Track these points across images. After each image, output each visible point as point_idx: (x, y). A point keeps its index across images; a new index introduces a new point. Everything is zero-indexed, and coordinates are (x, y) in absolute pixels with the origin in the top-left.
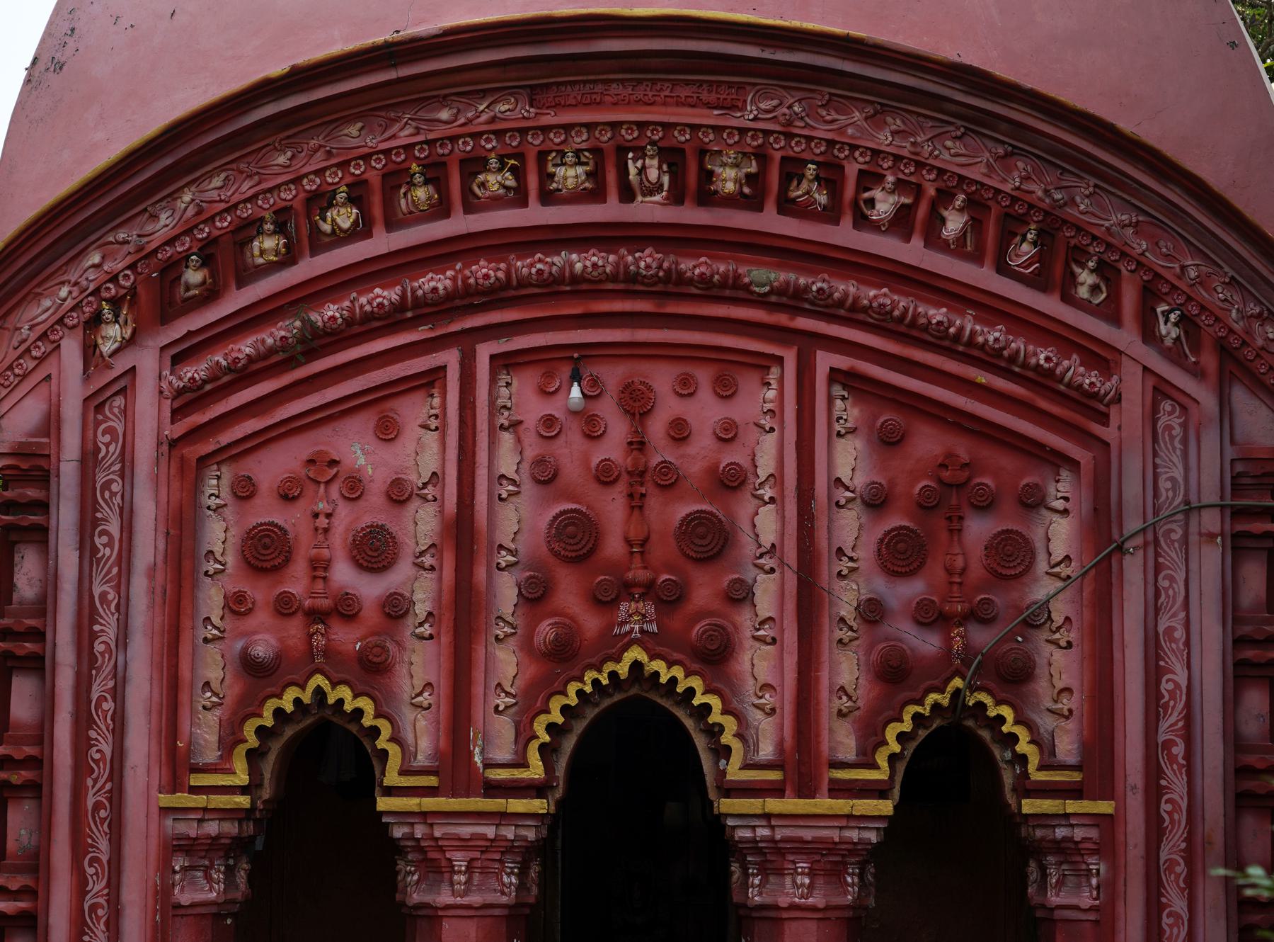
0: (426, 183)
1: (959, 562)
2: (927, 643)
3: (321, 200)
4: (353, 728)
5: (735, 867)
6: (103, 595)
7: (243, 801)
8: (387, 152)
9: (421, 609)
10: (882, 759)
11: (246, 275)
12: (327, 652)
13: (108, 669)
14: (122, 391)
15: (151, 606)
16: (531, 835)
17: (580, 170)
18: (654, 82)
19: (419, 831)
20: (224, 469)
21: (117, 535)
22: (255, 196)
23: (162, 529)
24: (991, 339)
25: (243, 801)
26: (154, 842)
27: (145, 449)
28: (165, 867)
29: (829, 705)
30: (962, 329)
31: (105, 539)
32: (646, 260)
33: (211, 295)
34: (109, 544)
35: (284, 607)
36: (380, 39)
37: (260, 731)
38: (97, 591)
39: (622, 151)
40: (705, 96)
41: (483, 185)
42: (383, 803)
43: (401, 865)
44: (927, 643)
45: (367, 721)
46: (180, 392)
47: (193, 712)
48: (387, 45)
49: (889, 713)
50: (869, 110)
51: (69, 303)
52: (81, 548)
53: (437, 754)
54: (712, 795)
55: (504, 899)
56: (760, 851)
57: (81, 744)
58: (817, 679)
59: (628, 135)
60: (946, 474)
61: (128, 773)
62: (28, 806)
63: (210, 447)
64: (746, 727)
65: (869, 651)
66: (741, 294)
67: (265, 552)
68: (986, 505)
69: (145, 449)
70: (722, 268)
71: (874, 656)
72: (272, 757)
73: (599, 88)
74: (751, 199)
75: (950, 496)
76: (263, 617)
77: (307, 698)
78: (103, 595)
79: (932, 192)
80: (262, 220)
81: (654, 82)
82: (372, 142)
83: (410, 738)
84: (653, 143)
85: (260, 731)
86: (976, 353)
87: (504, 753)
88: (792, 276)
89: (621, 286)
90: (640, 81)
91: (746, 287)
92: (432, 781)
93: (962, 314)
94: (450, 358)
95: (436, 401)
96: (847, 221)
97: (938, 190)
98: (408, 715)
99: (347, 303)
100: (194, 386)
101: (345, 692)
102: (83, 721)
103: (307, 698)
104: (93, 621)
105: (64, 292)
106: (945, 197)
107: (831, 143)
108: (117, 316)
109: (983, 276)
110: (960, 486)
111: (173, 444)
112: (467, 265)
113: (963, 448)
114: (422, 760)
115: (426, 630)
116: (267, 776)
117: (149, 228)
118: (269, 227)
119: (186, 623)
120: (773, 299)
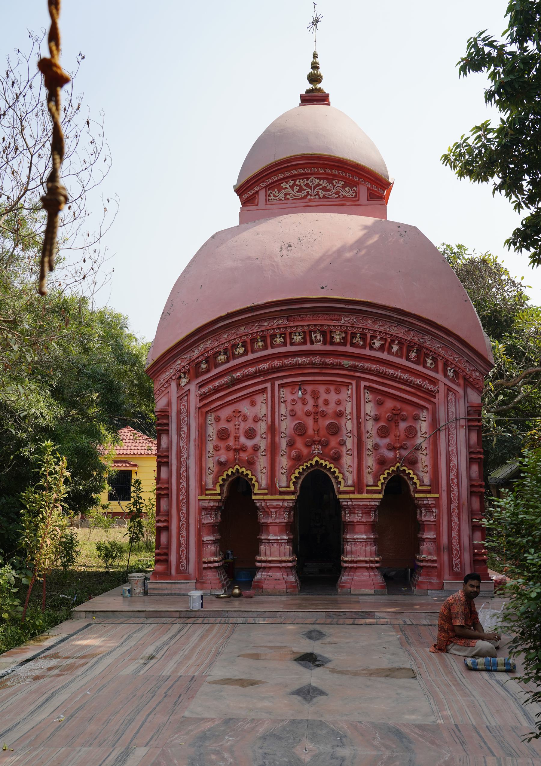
0: (261, 341)
1: (398, 434)
2: (390, 455)
3: (235, 346)
4: (246, 478)
5: (343, 512)
6: (183, 446)
7: (219, 497)
8: (251, 334)
9: (262, 448)
10: (379, 484)
11: (216, 366)
12: (239, 460)
13: (185, 465)
14: (187, 395)
15: (195, 449)
16: (291, 504)
17: (300, 337)
18: (318, 314)
19: (263, 504)
20: (212, 414)
21: (186, 431)
22: (219, 346)
23: (197, 429)
25: (219, 497)
26: (197, 507)
27: (193, 410)
28: (200, 514)
29: (365, 470)
30: (398, 375)
31: (183, 432)
32: (317, 359)
33: (208, 371)
34: (184, 434)
35: (228, 448)
36: (249, 305)
37: (223, 480)
38: (181, 445)
39: (310, 332)
40: (331, 318)
41: (275, 341)
42: (254, 497)
43: (259, 513)
44: (390, 455)
45: (250, 477)
46: (201, 395)
47: (206, 475)
48: (251, 307)
49: (381, 472)
50: (373, 320)
51: (173, 373)
52: (177, 435)
53: (267, 484)
54: (336, 494)
55: (285, 521)
56: (349, 508)
57: (178, 484)
58: (363, 464)
59: (312, 328)
60: (394, 412)
61: (190, 490)
62: (166, 499)
63: (209, 409)
64: (345, 476)
65: (375, 457)
66: (341, 367)
67: (223, 435)
68: (404, 419)
69: (193, 410)
70: (336, 361)
71: (377, 458)
72: (226, 486)
73: (304, 316)
74: (344, 344)
75: (395, 417)
76: (223, 451)
77: (234, 471)
78: (183, 446)
79: (389, 340)
80: (220, 351)
81: (318, 314)
82: (248, 331)
83: (260, 481)
84: (318, 330)
85: (223, 480)
87: (284, 484)
88: (354, 363)
89: (311, 366)
90: (315, 314)
91: (343, 366)
92: (266, 491)
93: (398, 371)
94: (268, 385)
95: (265, 396)
96: (368, 348)
98: (260, 475)
99: (242, 372)
100: (204, 394)
101: (244, 469)
102: (179, 478)
103: (234, 471)
104: (181, 453)
105: (171, 371)
106: (393, 341)
107: (363, 329)
108: (185, 376)
110: (398, 415)
111: (200, 408)
112: (272, 362)
113: (398, 405)
114: (263, 486)
115: (264, 453)
116: (225, 491)
117: (192, 354)
118: (222, 353)
119: (204, 453)
120: (349, 368)
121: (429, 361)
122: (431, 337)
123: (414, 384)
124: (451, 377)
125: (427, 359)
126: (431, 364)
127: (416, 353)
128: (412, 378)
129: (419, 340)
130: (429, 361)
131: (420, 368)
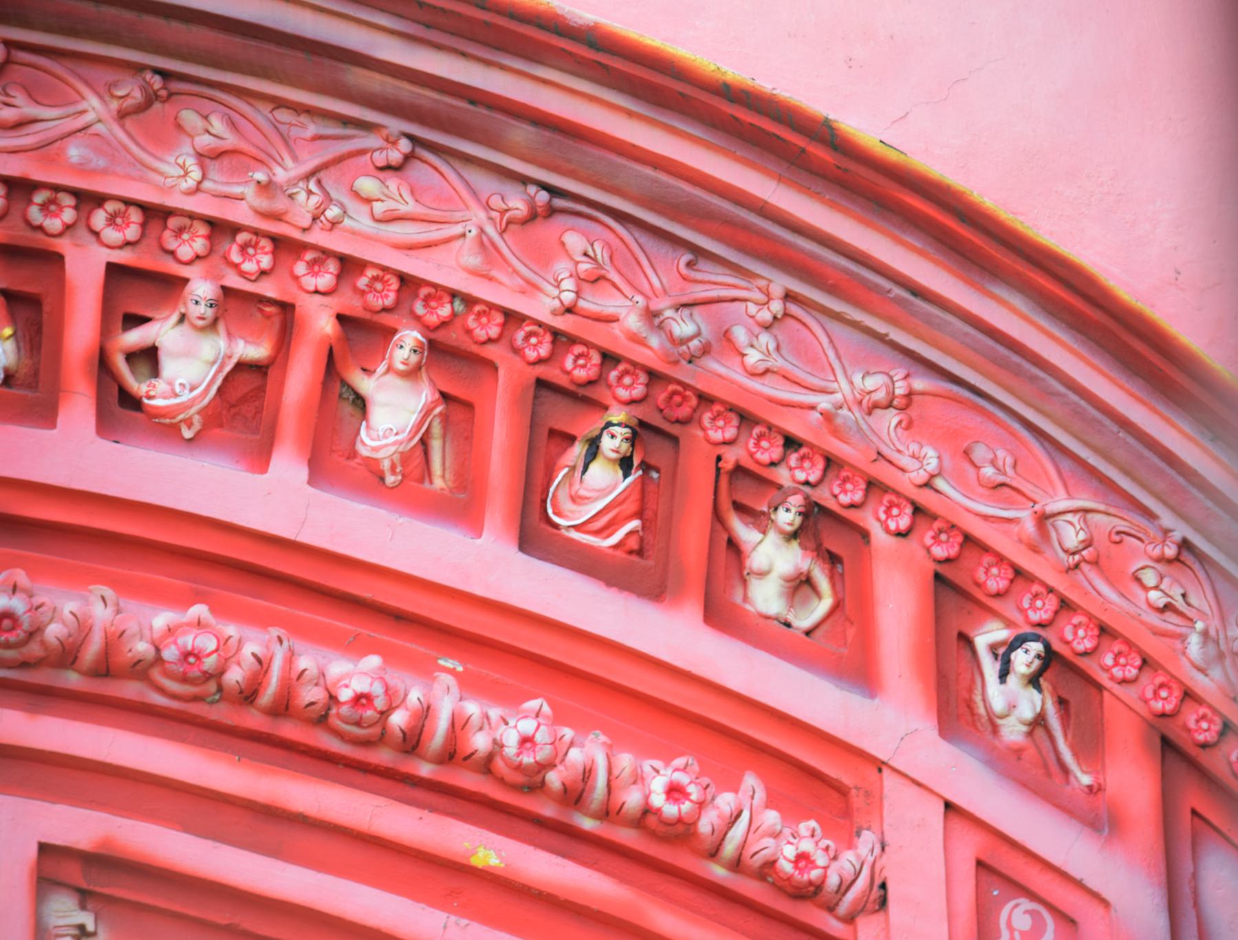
24: (511, 740)
30: (425, 713)
86: (469, 781)
97: (341, 318)
106: (362, 333)
109: (481, 562)
121: (773, 556)
122: (781, 282)
123: (608, 813)
124: (1013, 731)
125: (745, 533)
126: (801, 585)
127: (625, 464)
128: (588, 751)
129: (651, 315)
130: (773, 556)
131: (670, 633)
